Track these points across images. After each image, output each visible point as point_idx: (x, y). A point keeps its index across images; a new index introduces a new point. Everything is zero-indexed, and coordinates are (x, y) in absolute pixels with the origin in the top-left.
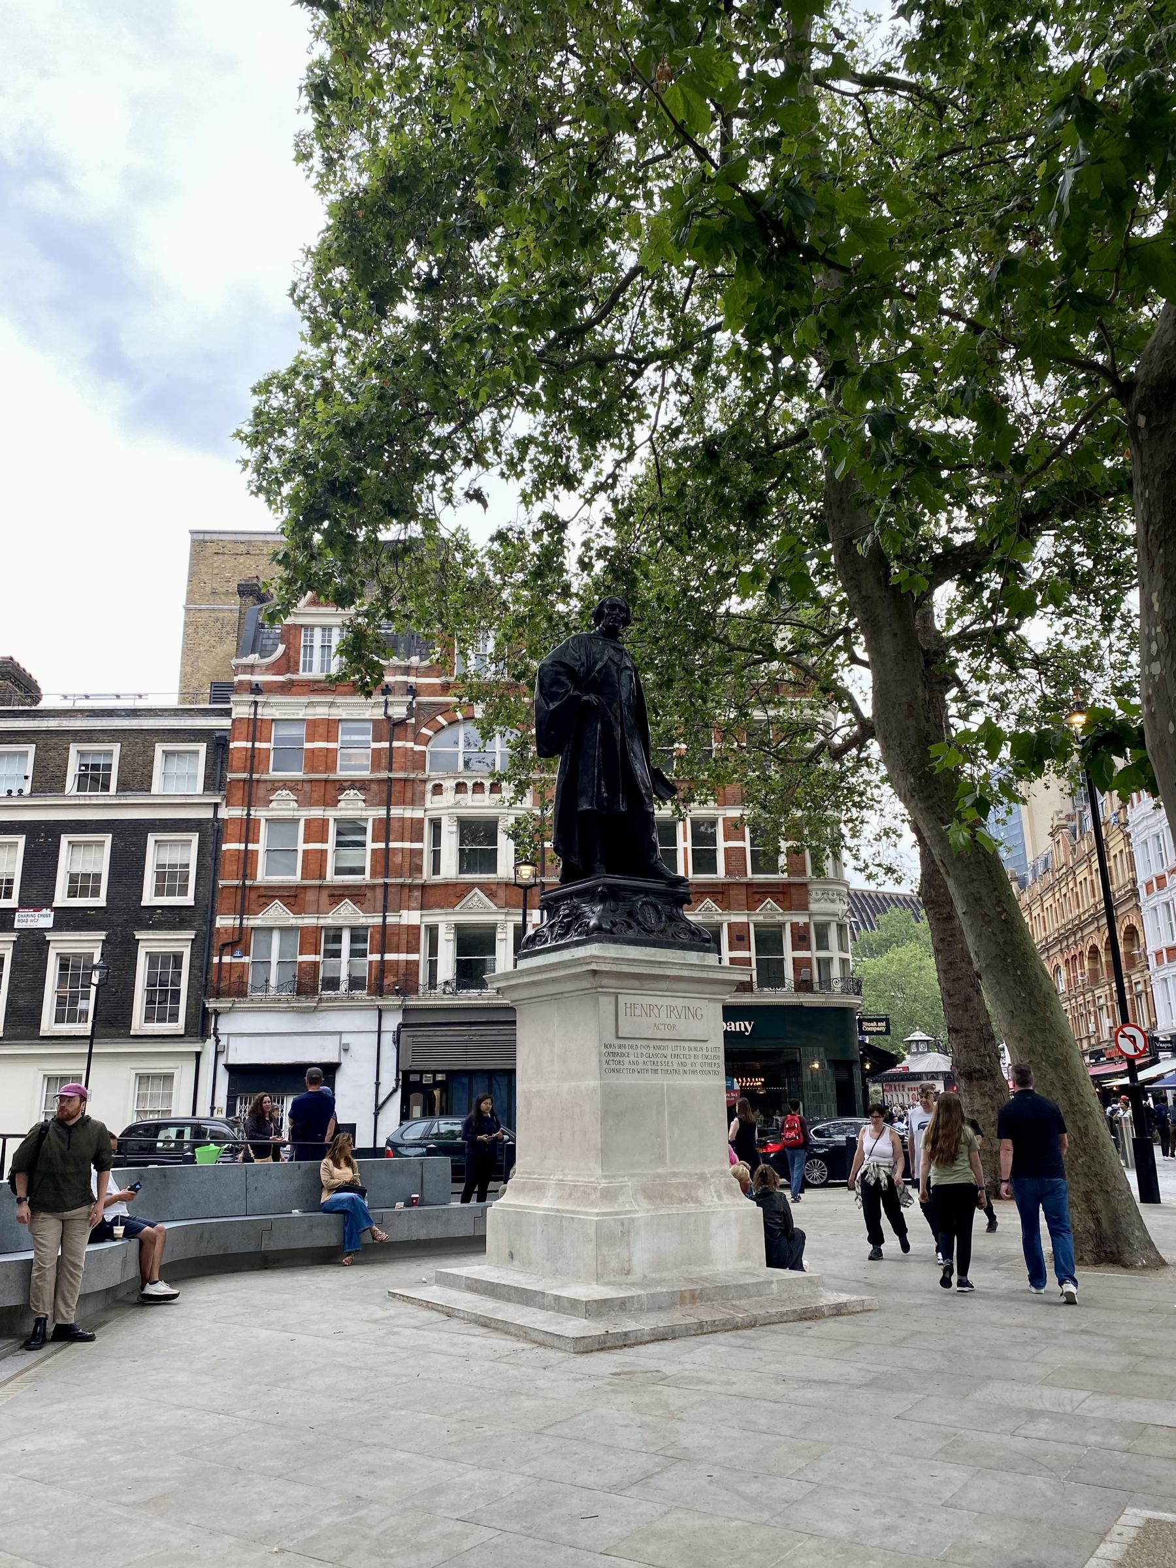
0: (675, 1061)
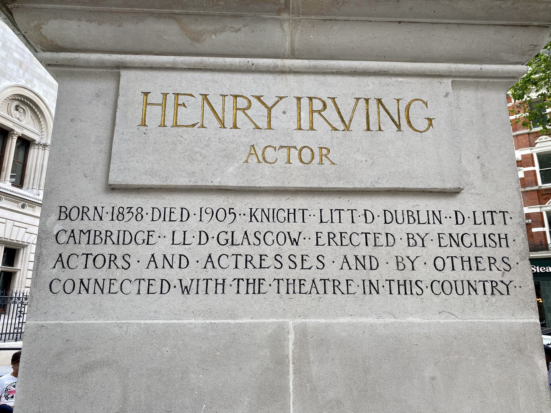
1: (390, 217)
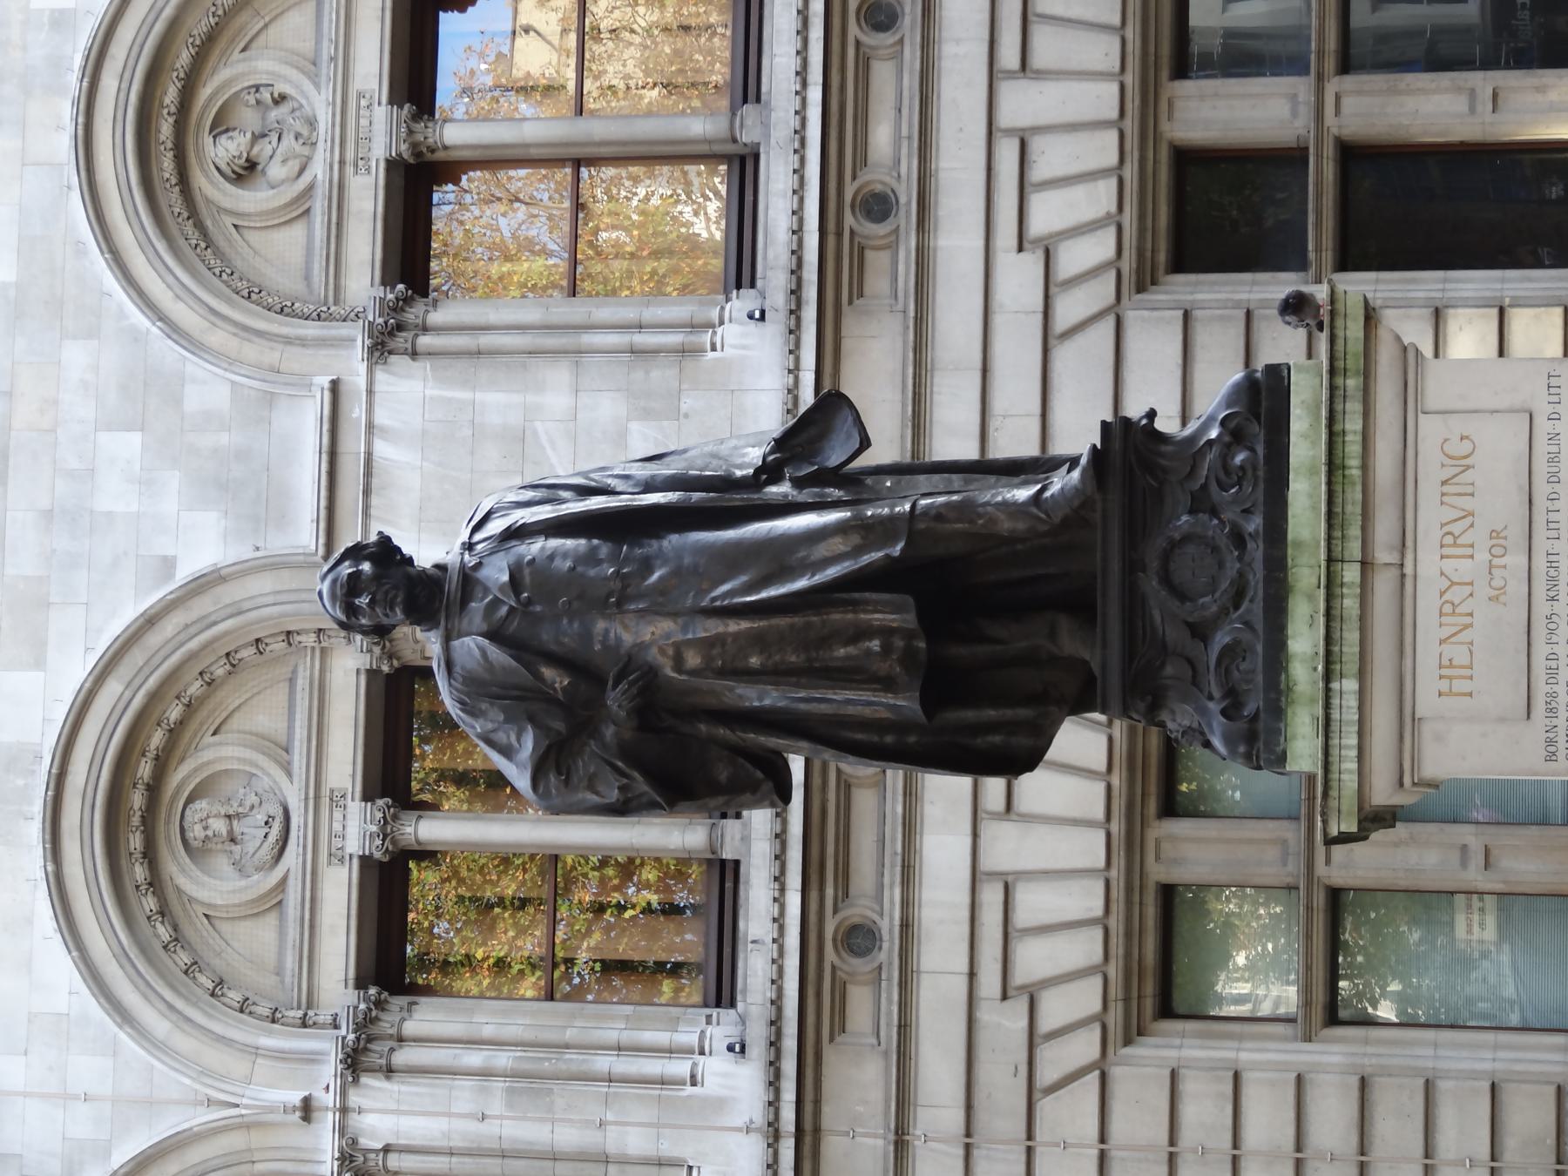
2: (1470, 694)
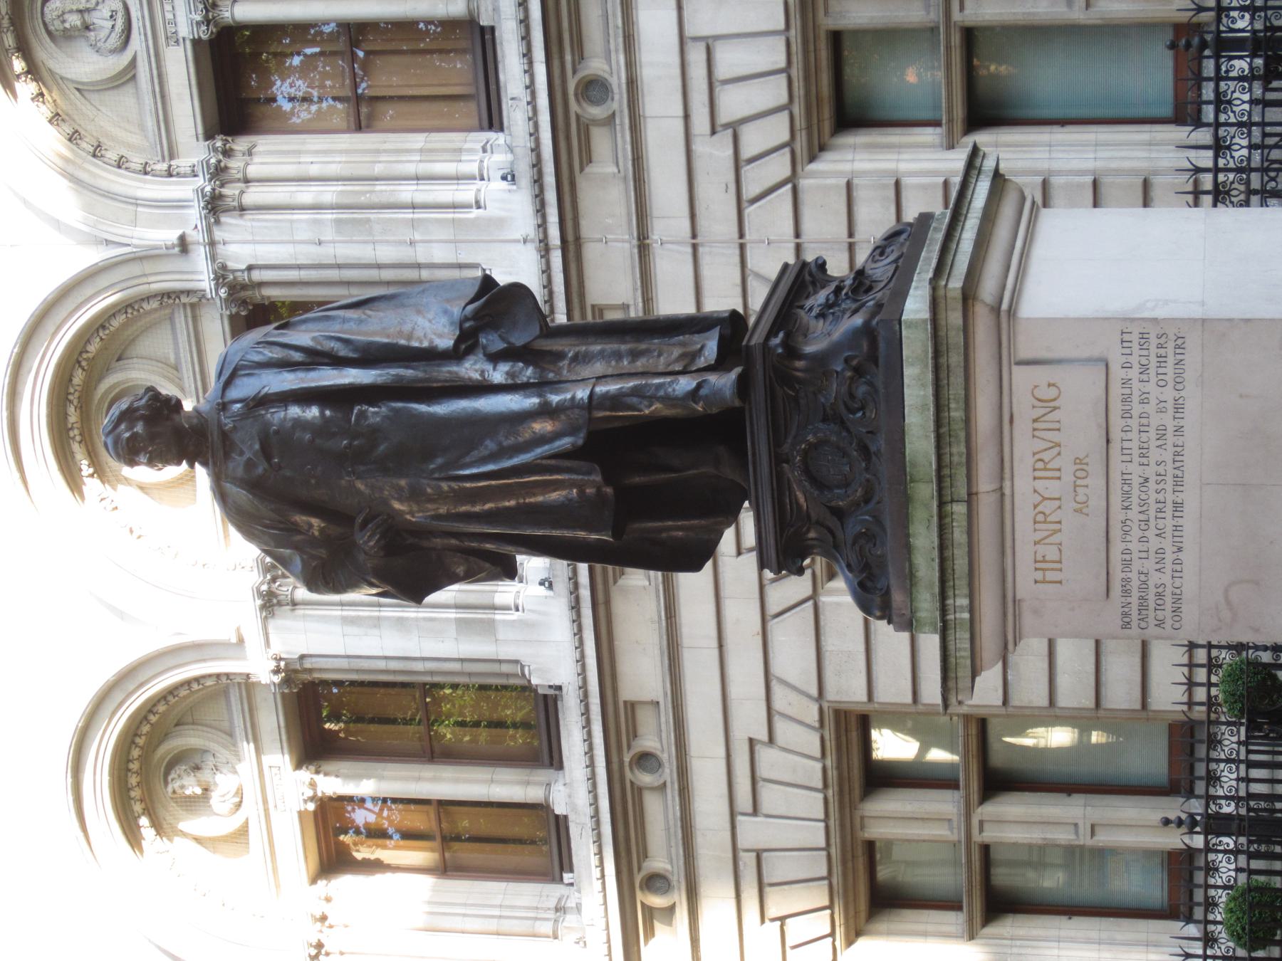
0: (1155, 455)
1: (1126, 414)
2: (1060, 582)
